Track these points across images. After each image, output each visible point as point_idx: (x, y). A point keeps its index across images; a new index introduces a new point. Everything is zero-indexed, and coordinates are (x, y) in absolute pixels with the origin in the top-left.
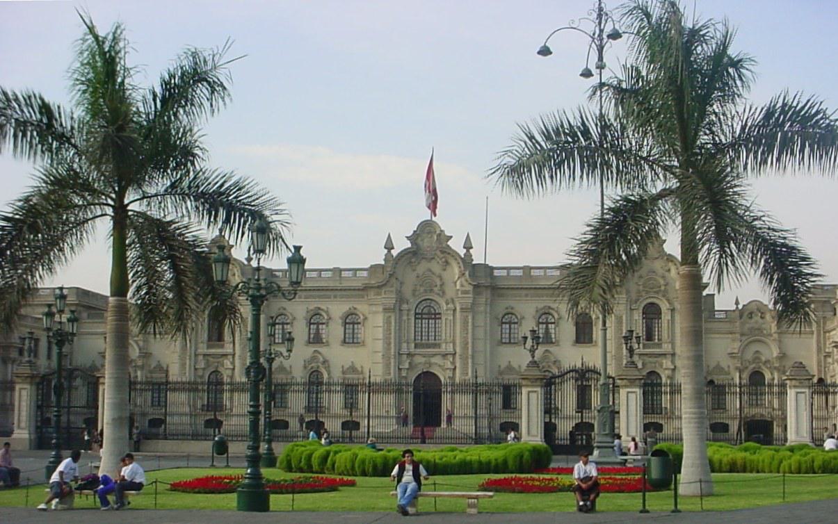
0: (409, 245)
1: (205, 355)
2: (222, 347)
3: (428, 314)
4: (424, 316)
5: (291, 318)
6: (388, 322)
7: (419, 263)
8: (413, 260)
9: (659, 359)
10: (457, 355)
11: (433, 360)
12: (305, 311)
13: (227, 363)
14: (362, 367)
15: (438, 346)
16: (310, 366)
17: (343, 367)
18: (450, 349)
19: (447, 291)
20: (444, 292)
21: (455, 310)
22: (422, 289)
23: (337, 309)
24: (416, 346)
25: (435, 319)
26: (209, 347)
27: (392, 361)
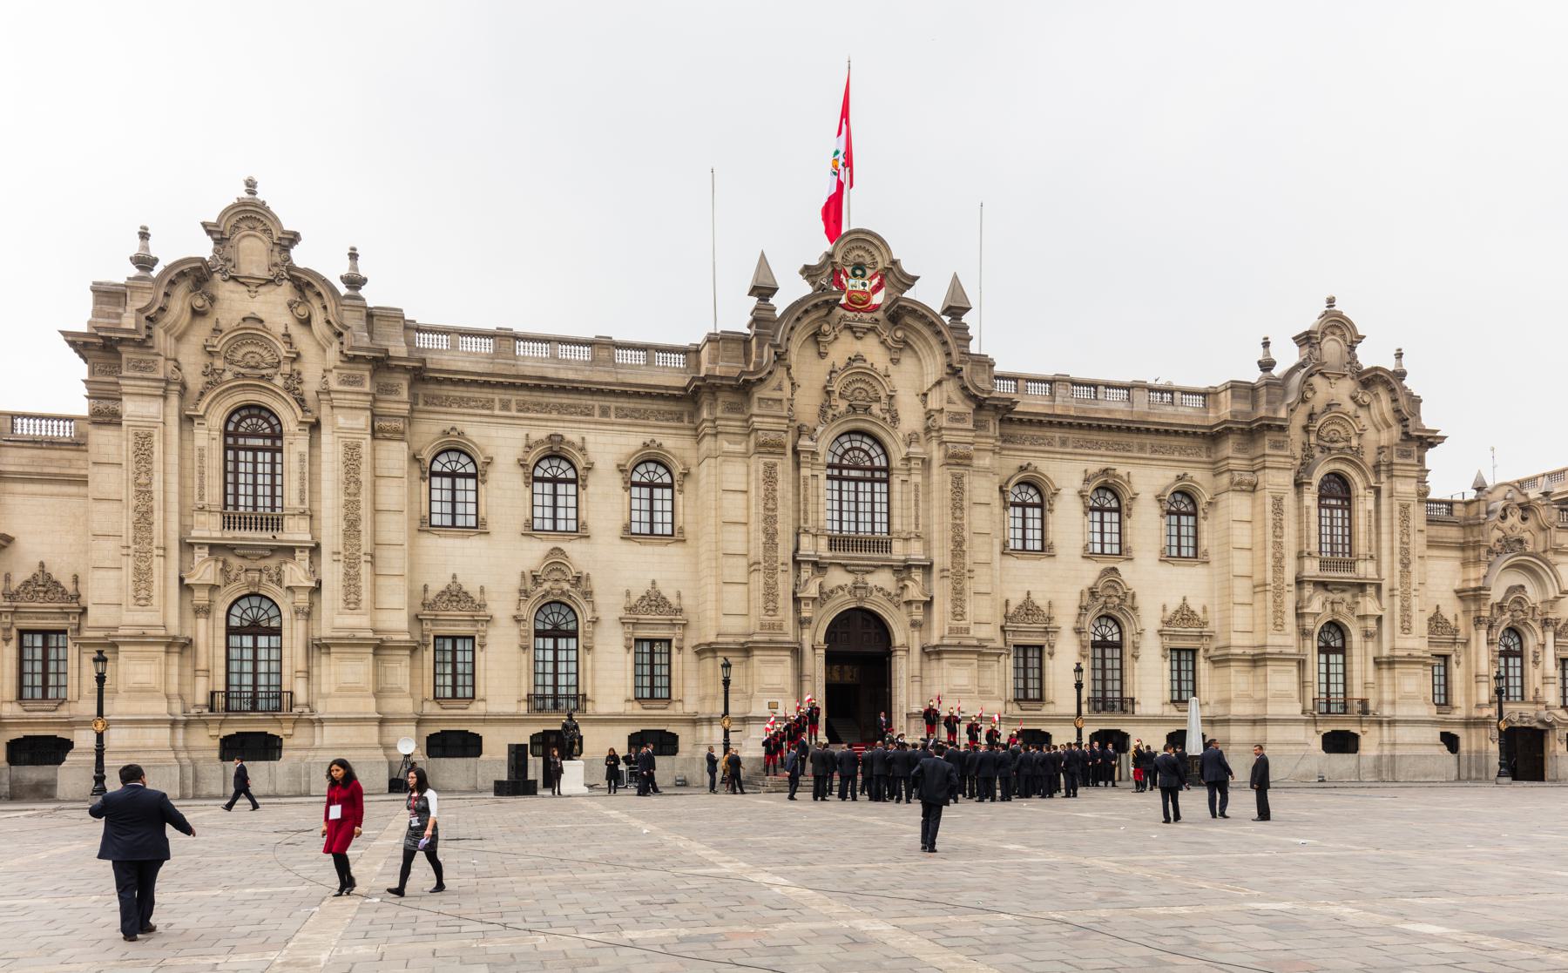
0: (807, 289)
1: (214, 548)
2: (275, 523)
3: (864, 461)
4: (845, 473)
5: (480, 460)
6: (770, 477)
7: (836, 338)
8: (826, 327)
9: (1348, 596)
10: (936, 569)
11: (875, 580)
12: (522, 443)
13: (296, 572)
14: (679, 596)
15: (886, 546)
16: (540, 591)
17: (628, 594)
18: (916, 551)
19: (902, 415)
20: (895, 419)
21: (926, 463)
22: (843, 406)
23: (607, 444)
24: (833, 543)
25: (873, 481)
26: (229, 522)
27: (780, 577)
